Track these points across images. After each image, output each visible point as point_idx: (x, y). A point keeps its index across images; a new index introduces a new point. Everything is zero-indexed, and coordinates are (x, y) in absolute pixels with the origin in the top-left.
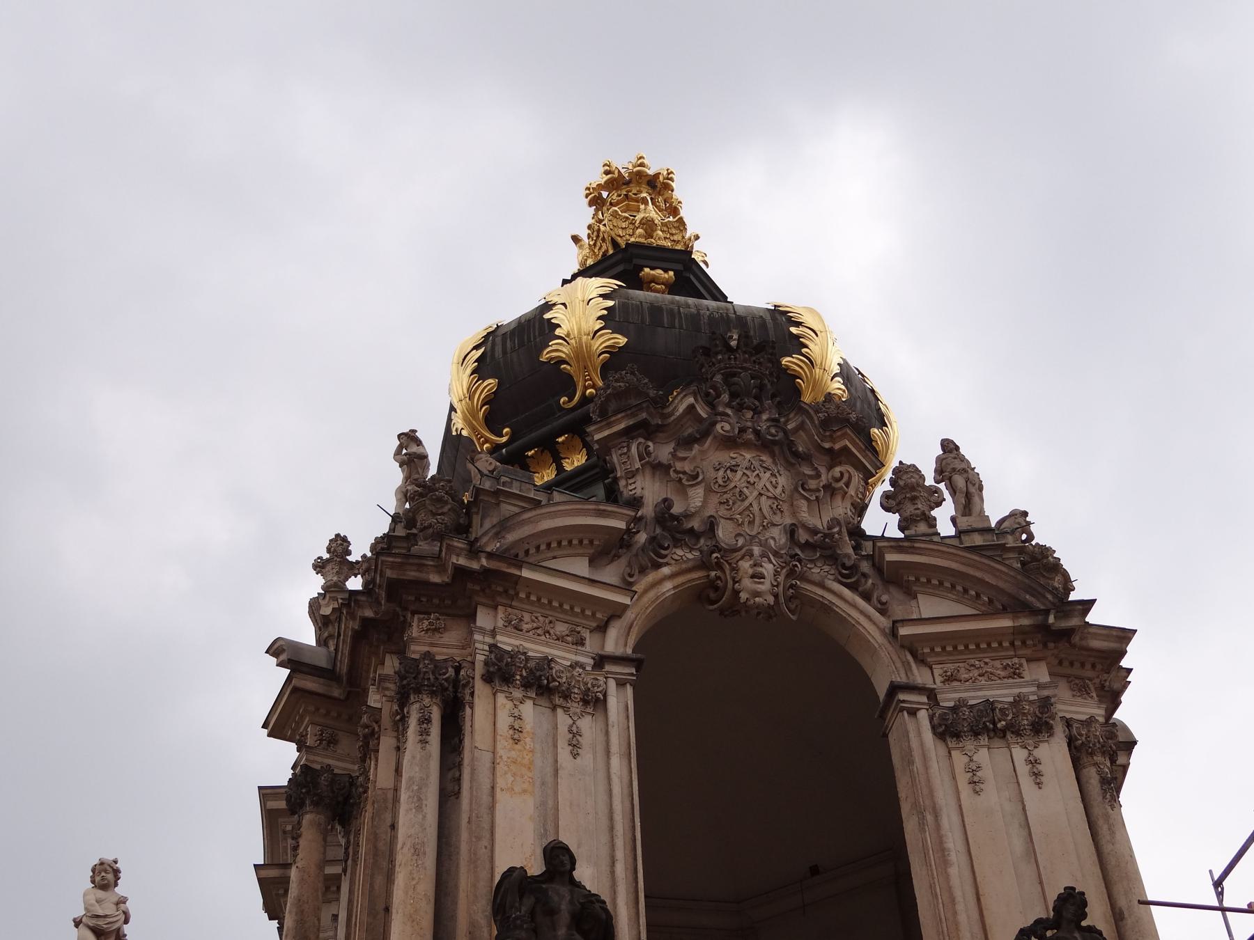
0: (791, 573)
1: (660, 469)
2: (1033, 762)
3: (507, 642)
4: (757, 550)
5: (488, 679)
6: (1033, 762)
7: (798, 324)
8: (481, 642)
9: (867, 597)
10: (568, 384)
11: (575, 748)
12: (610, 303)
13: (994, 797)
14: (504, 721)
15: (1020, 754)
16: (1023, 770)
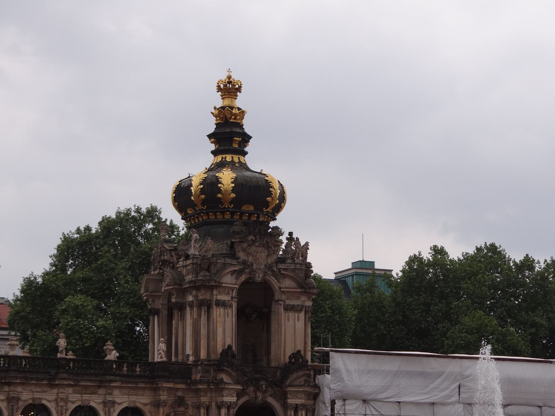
0: (265, 275)
1: (244, 250)
2: (298, 317)
3: (220, 297)
4: (260, 272)
5: (216, 305)
6: (298, 317)
7: (271, 187)
8: (215, 297)
9: (277, 279)
10: (222, 204)
11: (228, 316)
12: (233, 185)
13: (291, 323)
14: (218, 313)
15: (296, 315)
16: (296, 318)
